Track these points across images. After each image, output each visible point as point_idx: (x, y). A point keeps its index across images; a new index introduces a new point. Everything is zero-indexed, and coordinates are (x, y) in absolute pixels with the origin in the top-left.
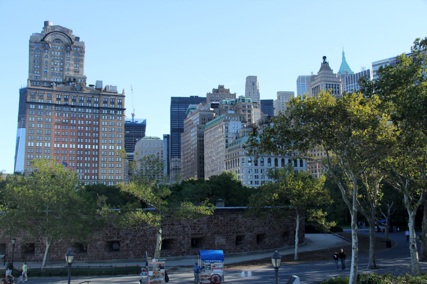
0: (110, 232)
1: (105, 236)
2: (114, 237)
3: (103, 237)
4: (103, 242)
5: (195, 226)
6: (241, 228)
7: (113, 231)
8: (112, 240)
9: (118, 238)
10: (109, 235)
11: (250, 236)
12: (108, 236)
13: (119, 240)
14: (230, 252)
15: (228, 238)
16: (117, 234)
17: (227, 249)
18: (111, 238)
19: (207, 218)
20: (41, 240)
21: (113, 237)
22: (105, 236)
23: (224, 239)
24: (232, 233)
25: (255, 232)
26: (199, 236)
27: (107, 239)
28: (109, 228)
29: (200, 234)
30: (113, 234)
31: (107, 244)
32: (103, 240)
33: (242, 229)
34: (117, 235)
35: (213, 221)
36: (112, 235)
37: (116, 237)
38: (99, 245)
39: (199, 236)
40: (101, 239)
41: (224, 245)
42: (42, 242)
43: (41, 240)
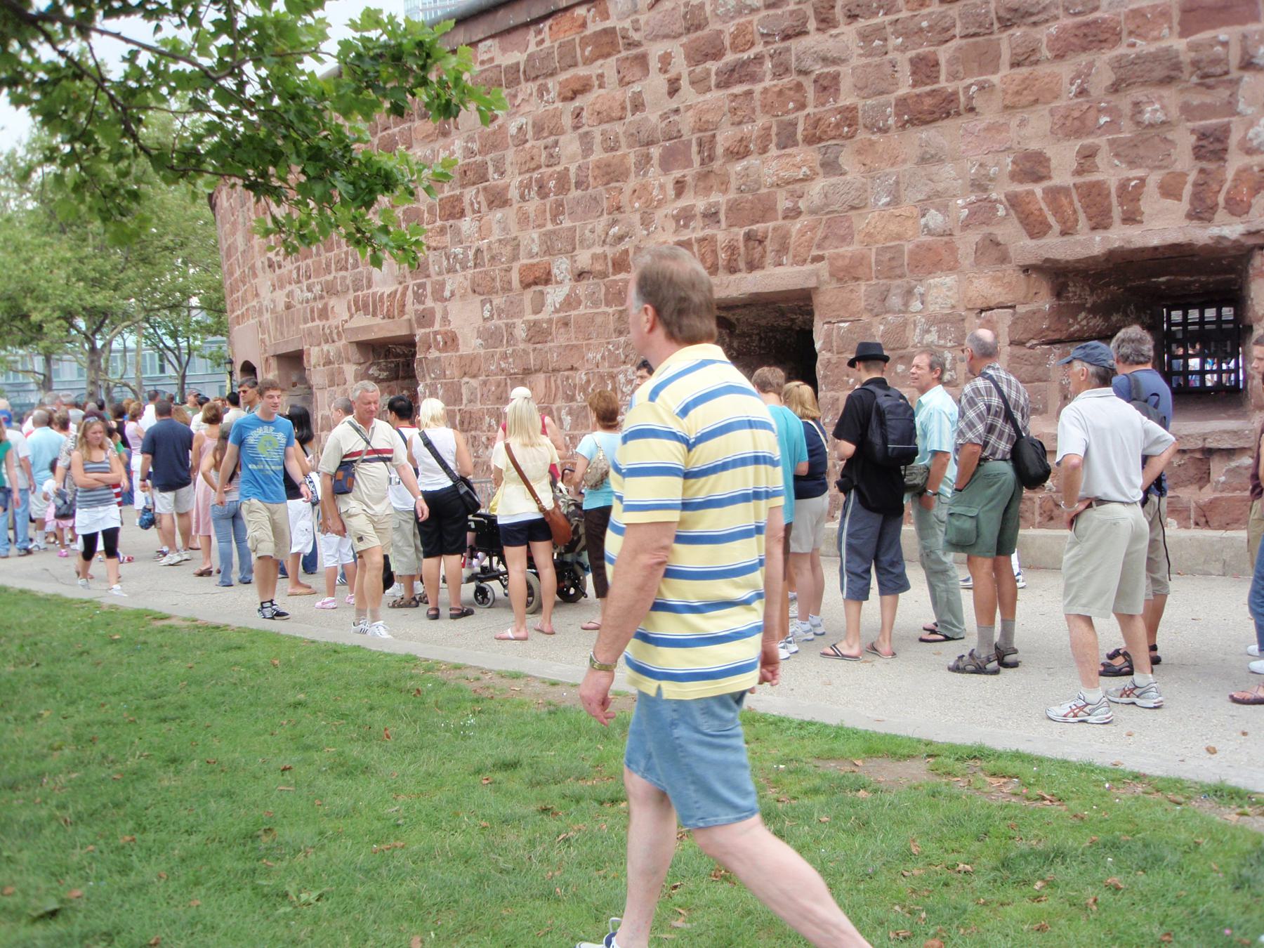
0: (1073, 126)
1: (1014, 202)
2: (1151, 202)
3: (982, 213)
4: (984, 286)
7: (1124, 102)
8: (1120, 236)
9: (1201, 211)
10: (1062, 176)
12: (1054, 194)
13: (1230, 229)
16: (1184, 140)
18: (1100, 222)
20: (438, 307)
21: (1131, 194)
22: (1014, 202)
27: (1035, 228)
28: (1065, 70)
30: (1127, 152)
31: (1045, 303)
32: (993, 250)
34: (1184, 161)
36: (1110, 173)
37: (1169, 190)
38: (933, 320)
40: (968, 242)
42: (445, 319)
43: (438, 307)
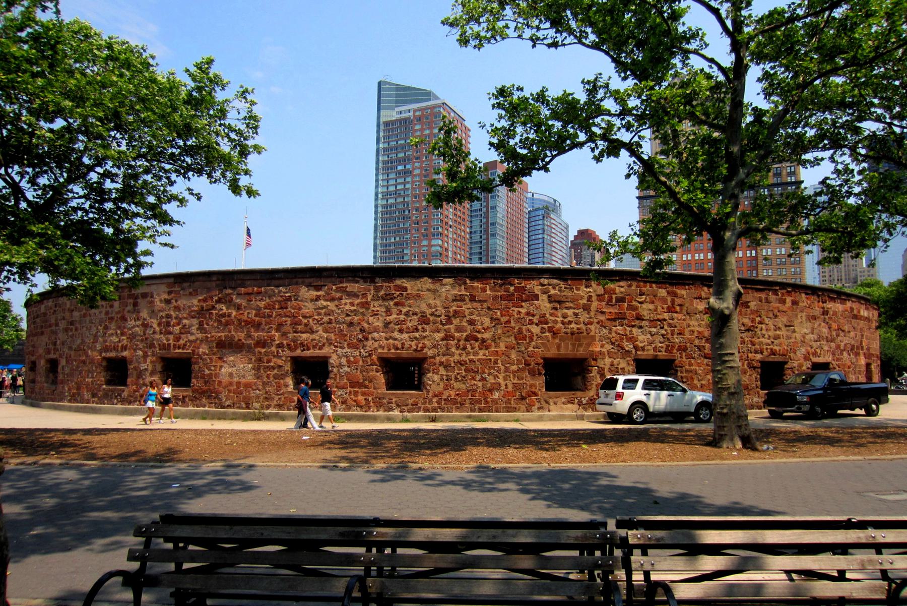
5: (168, 324)
6: (312, 332)
11: (349, 361)
14: (268, 407)
15: (260, 360)
17: (258, 397)
19: (199, 301)
23: (250, 366)
24: (273, 349)
25: (368, 349)
26: (177, 351)
29: (179, 348)
33: (314, 336)
35: (213, 308)
39: (177, 351)
41: (248, 385)
